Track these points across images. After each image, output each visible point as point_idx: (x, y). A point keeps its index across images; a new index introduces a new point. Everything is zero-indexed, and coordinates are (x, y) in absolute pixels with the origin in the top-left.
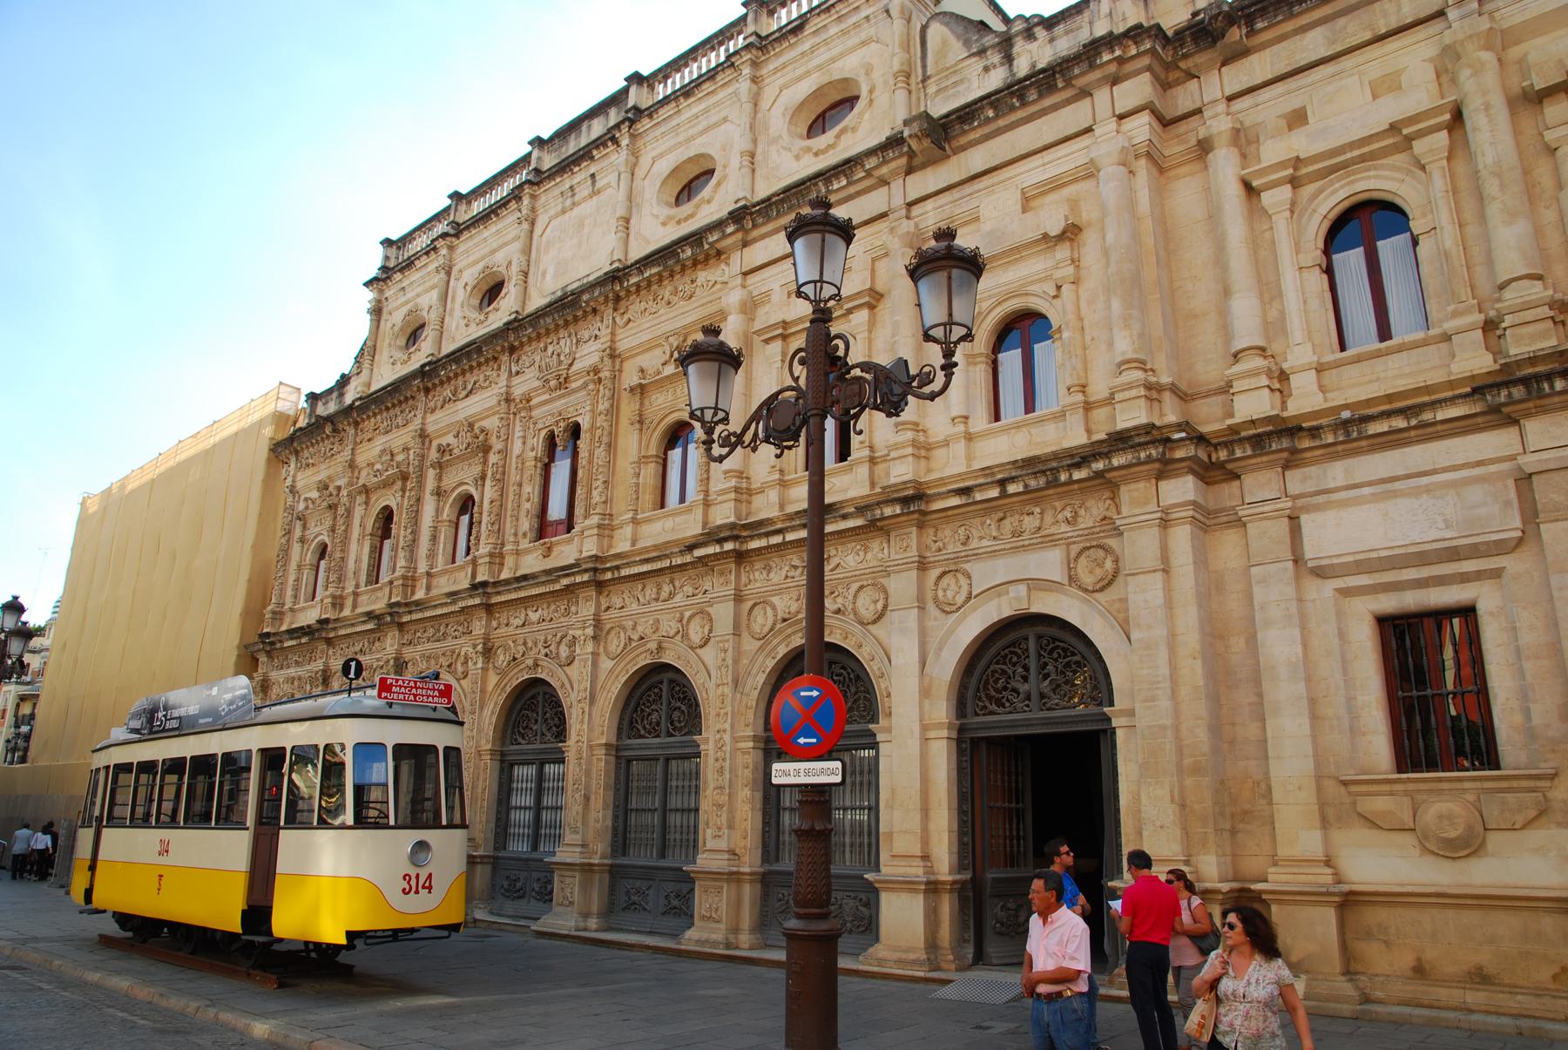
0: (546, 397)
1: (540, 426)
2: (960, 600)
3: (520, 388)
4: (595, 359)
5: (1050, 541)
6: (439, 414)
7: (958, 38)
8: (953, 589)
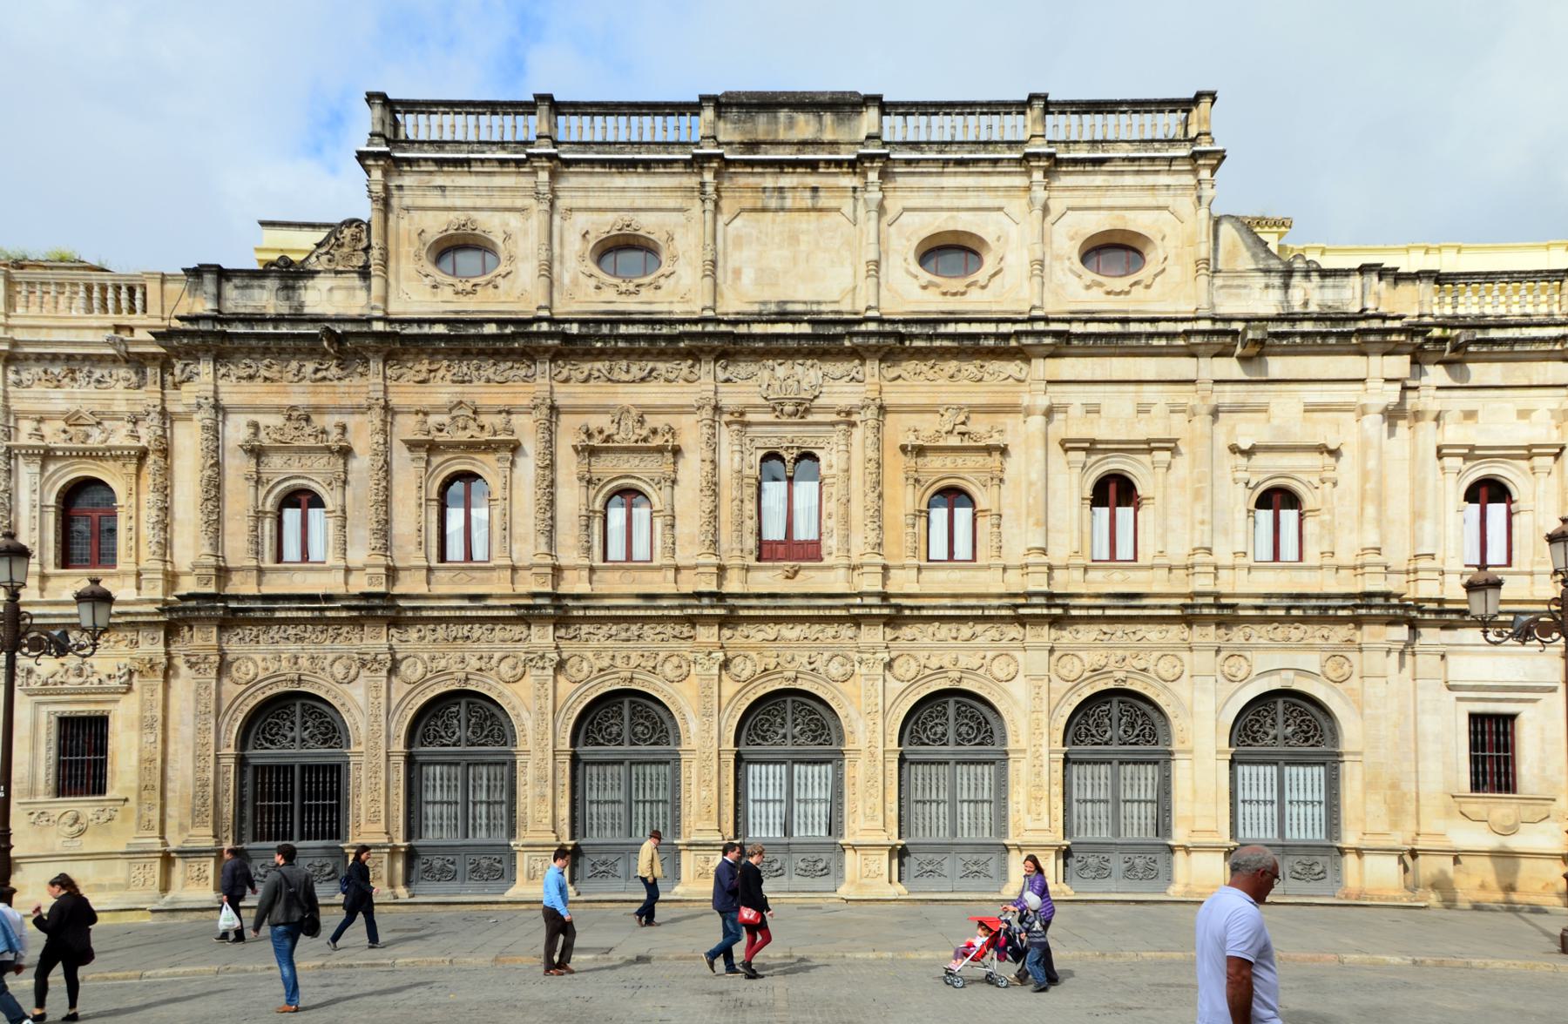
0: (770, 418)
2: (1241, 675)
3: (731, 398)
4: (856, 401)
5: (1310, 648)
6: (574, 388)
7: (1248, 248)
8: (1239, 667)
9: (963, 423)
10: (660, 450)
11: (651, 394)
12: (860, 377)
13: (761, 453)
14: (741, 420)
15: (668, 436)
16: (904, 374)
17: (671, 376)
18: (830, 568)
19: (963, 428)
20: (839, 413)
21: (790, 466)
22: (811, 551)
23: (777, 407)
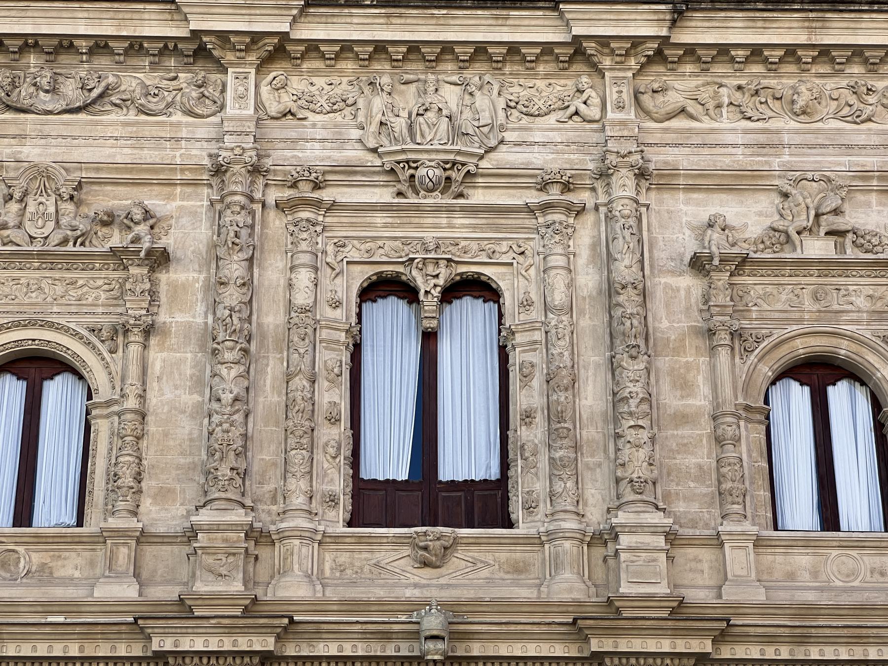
0: (385, 195)
1: (355, 256)
9: (837, 212)
10: (118, 257)
11: (103, 142)
12: (594, 112)
13: (360, 276)
14: (308, 192)
15: (142, 229)
16: (692, 107)
17: (153, 104)
18: (537, 541)
19: (840, 223)
20: (543, 187)
21: (430, 303)
22: (487, 504)
23: (402, 174)
